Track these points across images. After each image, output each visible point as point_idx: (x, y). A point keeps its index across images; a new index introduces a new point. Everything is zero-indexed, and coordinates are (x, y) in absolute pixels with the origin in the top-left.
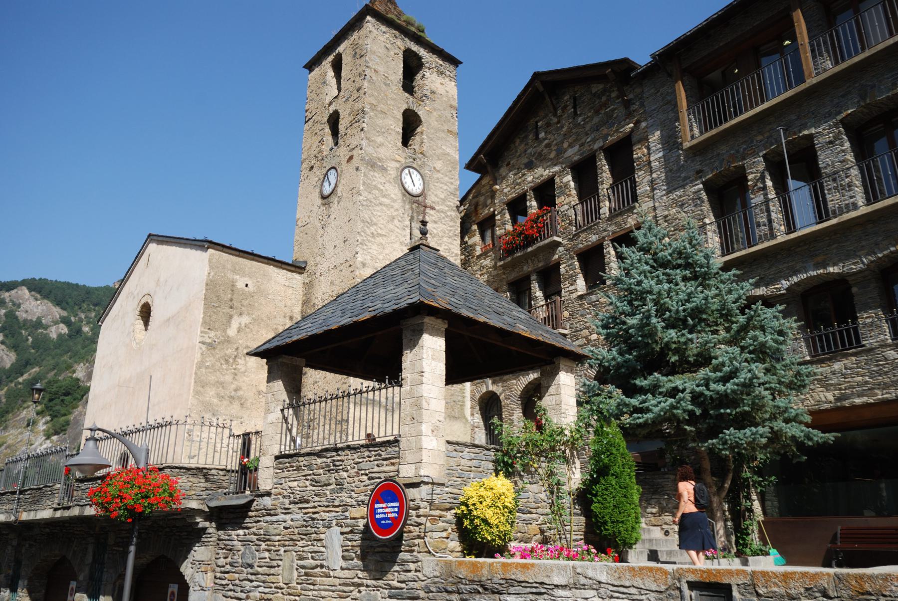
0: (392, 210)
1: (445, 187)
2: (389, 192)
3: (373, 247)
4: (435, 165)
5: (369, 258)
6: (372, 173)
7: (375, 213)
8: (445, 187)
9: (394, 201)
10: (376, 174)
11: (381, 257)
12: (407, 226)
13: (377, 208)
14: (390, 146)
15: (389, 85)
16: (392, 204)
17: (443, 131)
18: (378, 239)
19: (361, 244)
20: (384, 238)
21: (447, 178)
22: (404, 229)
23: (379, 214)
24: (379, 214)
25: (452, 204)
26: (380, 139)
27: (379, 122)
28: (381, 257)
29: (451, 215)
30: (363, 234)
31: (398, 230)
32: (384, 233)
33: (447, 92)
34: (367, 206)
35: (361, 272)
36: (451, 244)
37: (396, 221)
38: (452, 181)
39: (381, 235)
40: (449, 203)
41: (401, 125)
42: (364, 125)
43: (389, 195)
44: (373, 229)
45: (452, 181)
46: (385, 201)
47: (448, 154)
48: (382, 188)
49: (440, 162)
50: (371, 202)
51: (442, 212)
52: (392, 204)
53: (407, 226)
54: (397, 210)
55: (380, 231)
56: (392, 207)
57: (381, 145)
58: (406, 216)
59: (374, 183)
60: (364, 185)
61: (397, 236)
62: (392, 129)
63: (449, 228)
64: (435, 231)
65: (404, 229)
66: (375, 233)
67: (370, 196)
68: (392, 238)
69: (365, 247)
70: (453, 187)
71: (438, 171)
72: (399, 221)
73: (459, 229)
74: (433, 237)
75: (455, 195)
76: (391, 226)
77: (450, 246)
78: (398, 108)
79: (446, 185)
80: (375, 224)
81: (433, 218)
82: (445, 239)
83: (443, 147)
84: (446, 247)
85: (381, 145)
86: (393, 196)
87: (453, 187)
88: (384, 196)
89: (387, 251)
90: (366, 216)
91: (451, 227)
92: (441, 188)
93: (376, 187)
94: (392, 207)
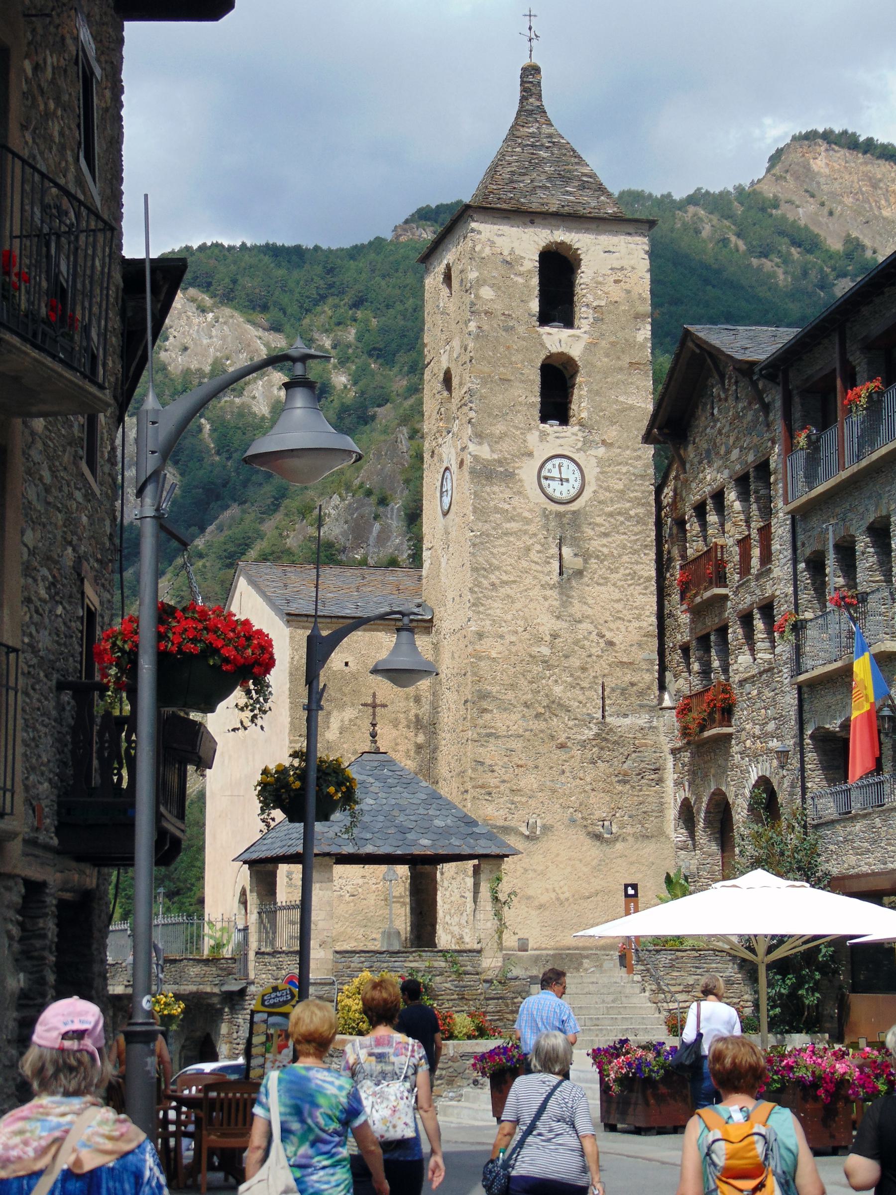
0: (526, 538)
1: (624, 470)
2: (520, 511)
3: (496, 605)
4: (605, 437)
5: (488, 622)
6: (488, 489)
7: (495, 551)
8: (624, 470)
9: (528, 521)
10: (496, 489)
11: (509, 617)
12: (552, 557)
13: (500, 542)
14: (518, 433)
15: (513, 328)
16: (526, 527)
17: (621, 369)
18: (502, 590)
19: (474, 605)
20: (513, 586)
21: (628, 452)
22: (549, 563)
23: (503, 550)
24: (503, 550)
25: (639, 494)
26: (499, 428)
27: (498, 400)
28: (509, 617)
29: (636, 514)
30: (476, 589)
31: (539, 568)
32: (512, 579)
33: (628, 292)
34: (482, 543)
35: (478, 647)
36: (637, 563)
37: (533, 555)
38: (639, 453)
39: (506, 583)
40: (632, 495)
41: (537, 388)
42: (472, 414)
43: (519, 515)
44: (493, 578)
45: (639, 453)
46: (513, 526)
47: (632, 408)
48: (506, 506)
49: (614, 427)
50: (488, 536)
51: (619, 513)
52: (526, 527)
53: (552, 557)
54: (535, 535)
55: (505, 578)
56: (526, 532)
57: (503, 436)
58: (550, 539)
59: (492, 504)
60: (474, 512)
61: (535, 578)
62: (521, 404)
63: (633, 538)
64: (605, 551)
65: (549, 563)
66: (497, 582)
67: (487, 526)
68: (527, 581)
69: (481, 609)
70: (639, 464)
71: (611, 444)
72: (538, 552)
73: (653, 534)
74: (602, 562)
75: (643, 477)
76: (524, 564)
77: (635, 567)
78: (531, 361)
79: (627, 464)
80: (498, 568)
81: (602, 529)
82: (625, 558)
83: (621, 399)
84: (627, 571)
85: (503, 436)
86: (526, 514)
87: (639, 464)
88: (512, 519)
89: (518, 605)
90: (481, 560)
91: (636, 534)
92: (617, 473)
93: (497, 510)
94: (526, 532)
